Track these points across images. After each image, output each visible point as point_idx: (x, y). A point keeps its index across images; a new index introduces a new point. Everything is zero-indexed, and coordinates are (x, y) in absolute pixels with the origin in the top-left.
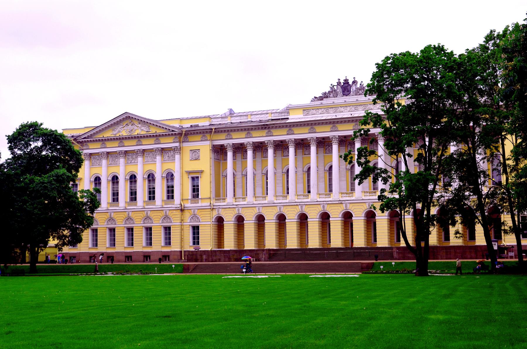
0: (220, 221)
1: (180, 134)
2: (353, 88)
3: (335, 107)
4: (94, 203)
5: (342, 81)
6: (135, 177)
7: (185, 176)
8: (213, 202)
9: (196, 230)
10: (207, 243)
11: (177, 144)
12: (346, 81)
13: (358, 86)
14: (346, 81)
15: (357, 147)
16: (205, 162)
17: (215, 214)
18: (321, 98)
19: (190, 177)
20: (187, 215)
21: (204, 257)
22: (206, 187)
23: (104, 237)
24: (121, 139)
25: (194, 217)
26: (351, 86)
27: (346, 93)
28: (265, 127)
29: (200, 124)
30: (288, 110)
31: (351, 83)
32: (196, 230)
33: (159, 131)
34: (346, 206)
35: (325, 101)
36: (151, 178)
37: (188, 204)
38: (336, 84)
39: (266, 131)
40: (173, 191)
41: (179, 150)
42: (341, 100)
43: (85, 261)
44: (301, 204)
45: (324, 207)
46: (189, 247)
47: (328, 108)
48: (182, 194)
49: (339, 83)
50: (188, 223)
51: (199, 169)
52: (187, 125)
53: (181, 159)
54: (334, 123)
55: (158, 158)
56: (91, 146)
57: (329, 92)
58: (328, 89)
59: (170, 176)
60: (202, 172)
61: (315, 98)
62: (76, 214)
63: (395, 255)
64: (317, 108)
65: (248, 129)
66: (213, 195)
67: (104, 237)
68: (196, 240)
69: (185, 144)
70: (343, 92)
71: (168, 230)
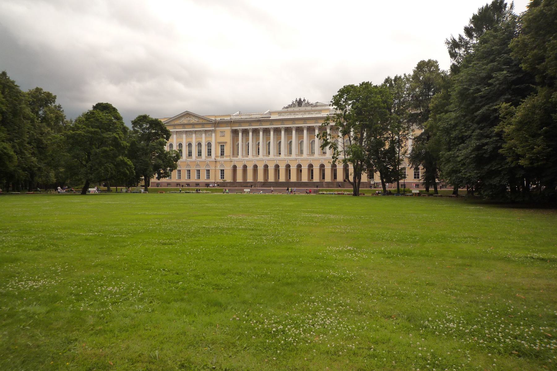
0: (235, 167)
1: (215, 123)
3: (294, 112)
4: (178, 156)
5: (298, 100)
6: (210, 143)
7: (217, 144)
9: (222, 171)
10: (228, 178)
11: (213, 128)
12: (300, 99)
14: (300, 99)
15: (323, 132)
16: (228, 138)
17: (232, 164)
18: (287, 108)
20: (218, 164)
21: (228, 185)
22: (228, 150)
23: (184, 175)
24: (184, 125)
25: (222, 165)
28: (259, 121)
29: (226, 118)
30: (270, 113)
32: (222, 171)
33: (204, 122)
35: (289, 109)
36: (200, 144)
37: (219, 159)
40: (211, 152)
41: (215, 131)
42: (297, 109)
43: (165, 186)
46: (219, 180)
47: (291, 112)
48: (216, 154)
49: (296, 100)
50: (219, 168)
51: (225, 141)
52: (218, 119)
53: (216, 136)
54: (305, 120)
55: (204, 135)
59: (209, 145)
60: (226, 143)
62: (169, 162)
63: (324, 185)
64: (285, 112)
65: (250, 122)
66: (231, 155)
67: (184, 175)
68: (222, 176)
69: (217, 129)
71: (208, 171)
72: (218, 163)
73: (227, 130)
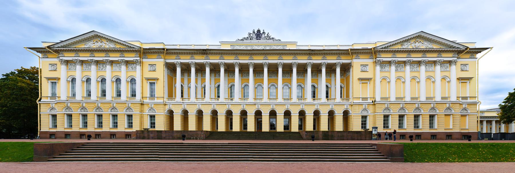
2: (263, 36)
7: (145, 81)
8: (166, 100)
12: (259, 31)
14: (259, 31)
16: (160, 73)
17: (167, 108)
19: (148, 82)
25: (151, 109)
27: (258, 38)
31: (261, 32)
37: (147, 101)
39: (205, 56)
41: (141, 63)
42: (255, 41)
49: (254, 32)
56: (66, 54)
58: (247, 36)
60: (157, 79)
66: (166, 95)
70: (257, 37)
72: (145, 106)
73: (160, 63)
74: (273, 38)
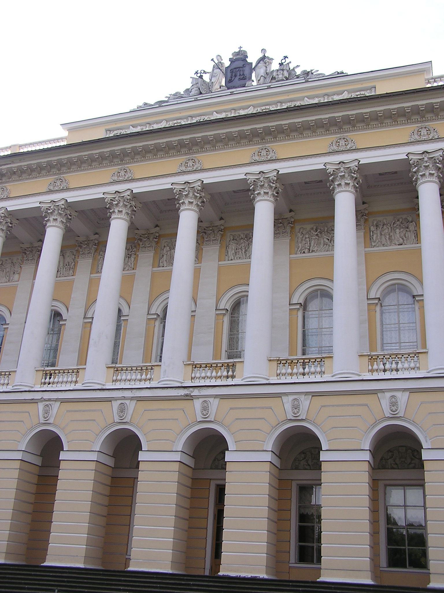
12: (240, 57)
13: (275, 66)
14: (240, 57)
26: (252, 70)
27: (236, 81)
31: (253, 58)
34: (205, 408)
38: (209, 68)
44: (46, 396)
45: (122, 409)
49: (218, 66)
57: (187, 90)
61: (145, 104)
74: (306, 73)
